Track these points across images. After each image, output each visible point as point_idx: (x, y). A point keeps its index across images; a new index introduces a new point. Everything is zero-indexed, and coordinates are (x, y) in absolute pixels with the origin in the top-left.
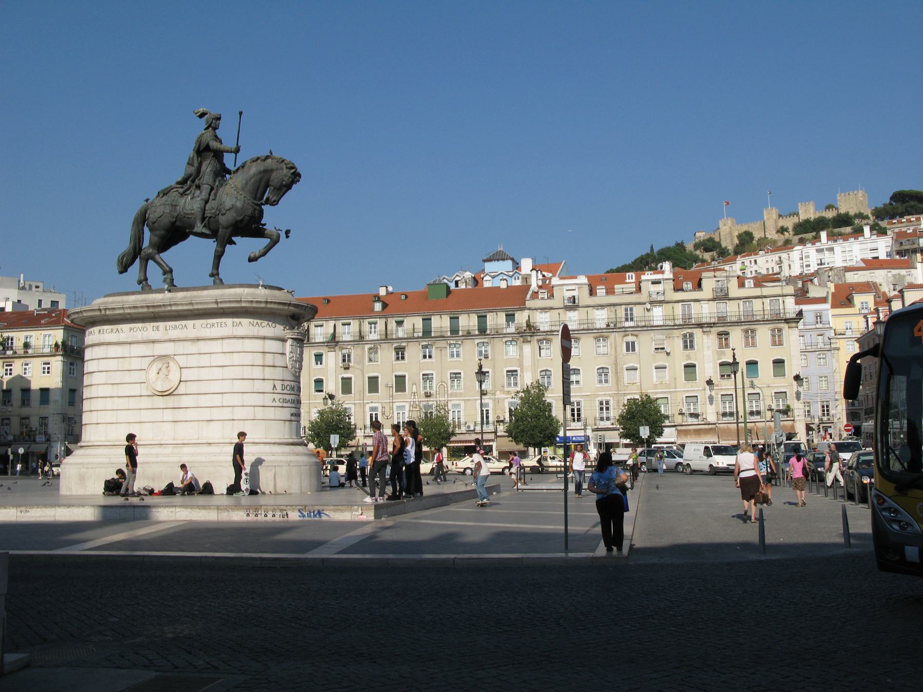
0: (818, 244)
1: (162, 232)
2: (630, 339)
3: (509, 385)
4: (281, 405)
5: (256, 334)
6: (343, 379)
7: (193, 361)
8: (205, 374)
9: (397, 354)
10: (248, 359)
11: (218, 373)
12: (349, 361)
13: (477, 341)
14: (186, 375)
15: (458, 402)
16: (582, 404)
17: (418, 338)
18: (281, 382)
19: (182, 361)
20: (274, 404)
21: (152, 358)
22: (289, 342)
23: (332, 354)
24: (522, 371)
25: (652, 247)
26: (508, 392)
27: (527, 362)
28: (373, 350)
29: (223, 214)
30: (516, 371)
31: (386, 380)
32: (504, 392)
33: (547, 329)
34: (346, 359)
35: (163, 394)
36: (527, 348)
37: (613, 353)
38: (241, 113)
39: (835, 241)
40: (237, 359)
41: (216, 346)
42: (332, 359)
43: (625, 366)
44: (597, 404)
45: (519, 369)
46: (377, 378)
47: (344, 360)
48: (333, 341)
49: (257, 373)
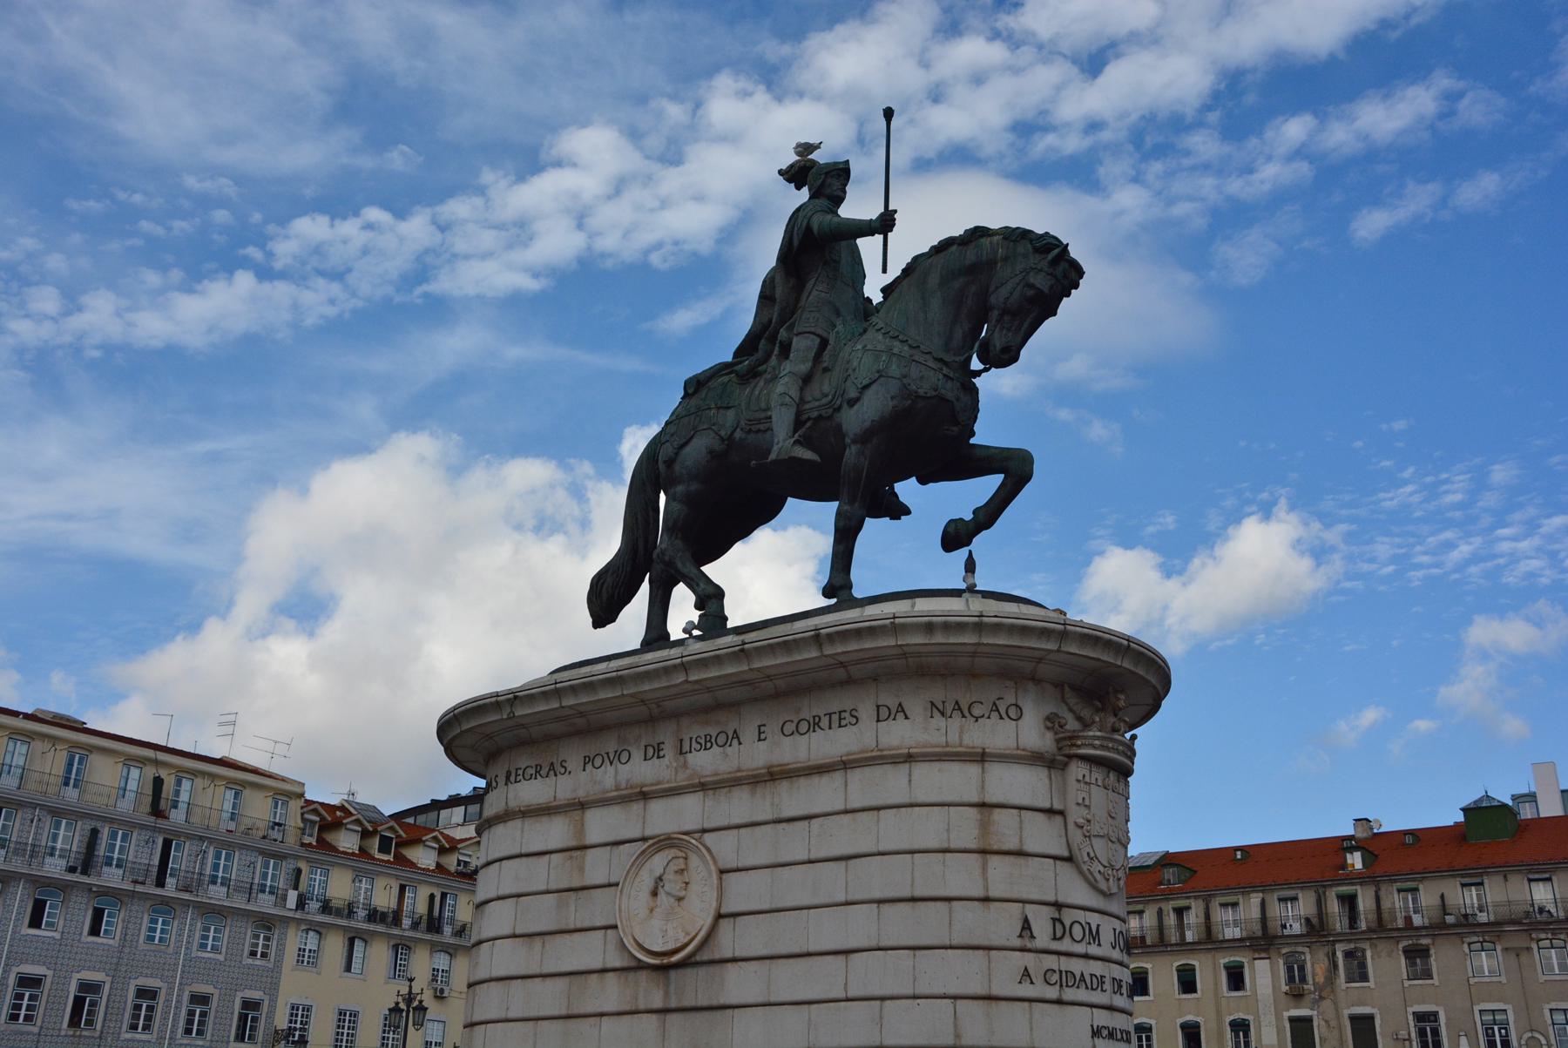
1: (694, 486)
4: (1052, 993)
5: (953, 737)
7: (757, 847)
8: (795, 887)
10: (927, 829)
11: (832, 882)
12: (1303, 979)
14: (745, 892)
18: (1048, 912)
19: (725, 847)
20: (1026, 990)
21: (640, 847)
22: (1078, 770)
23: (1262, 966)
29: (852, 403)
35: (665, 966)
38: (889, 114)
40: (893, 831)
41: (823, 794)
46: (1370, 1018)
47: (1291, 979)
48: (1264, 941)
49: (960, 876)
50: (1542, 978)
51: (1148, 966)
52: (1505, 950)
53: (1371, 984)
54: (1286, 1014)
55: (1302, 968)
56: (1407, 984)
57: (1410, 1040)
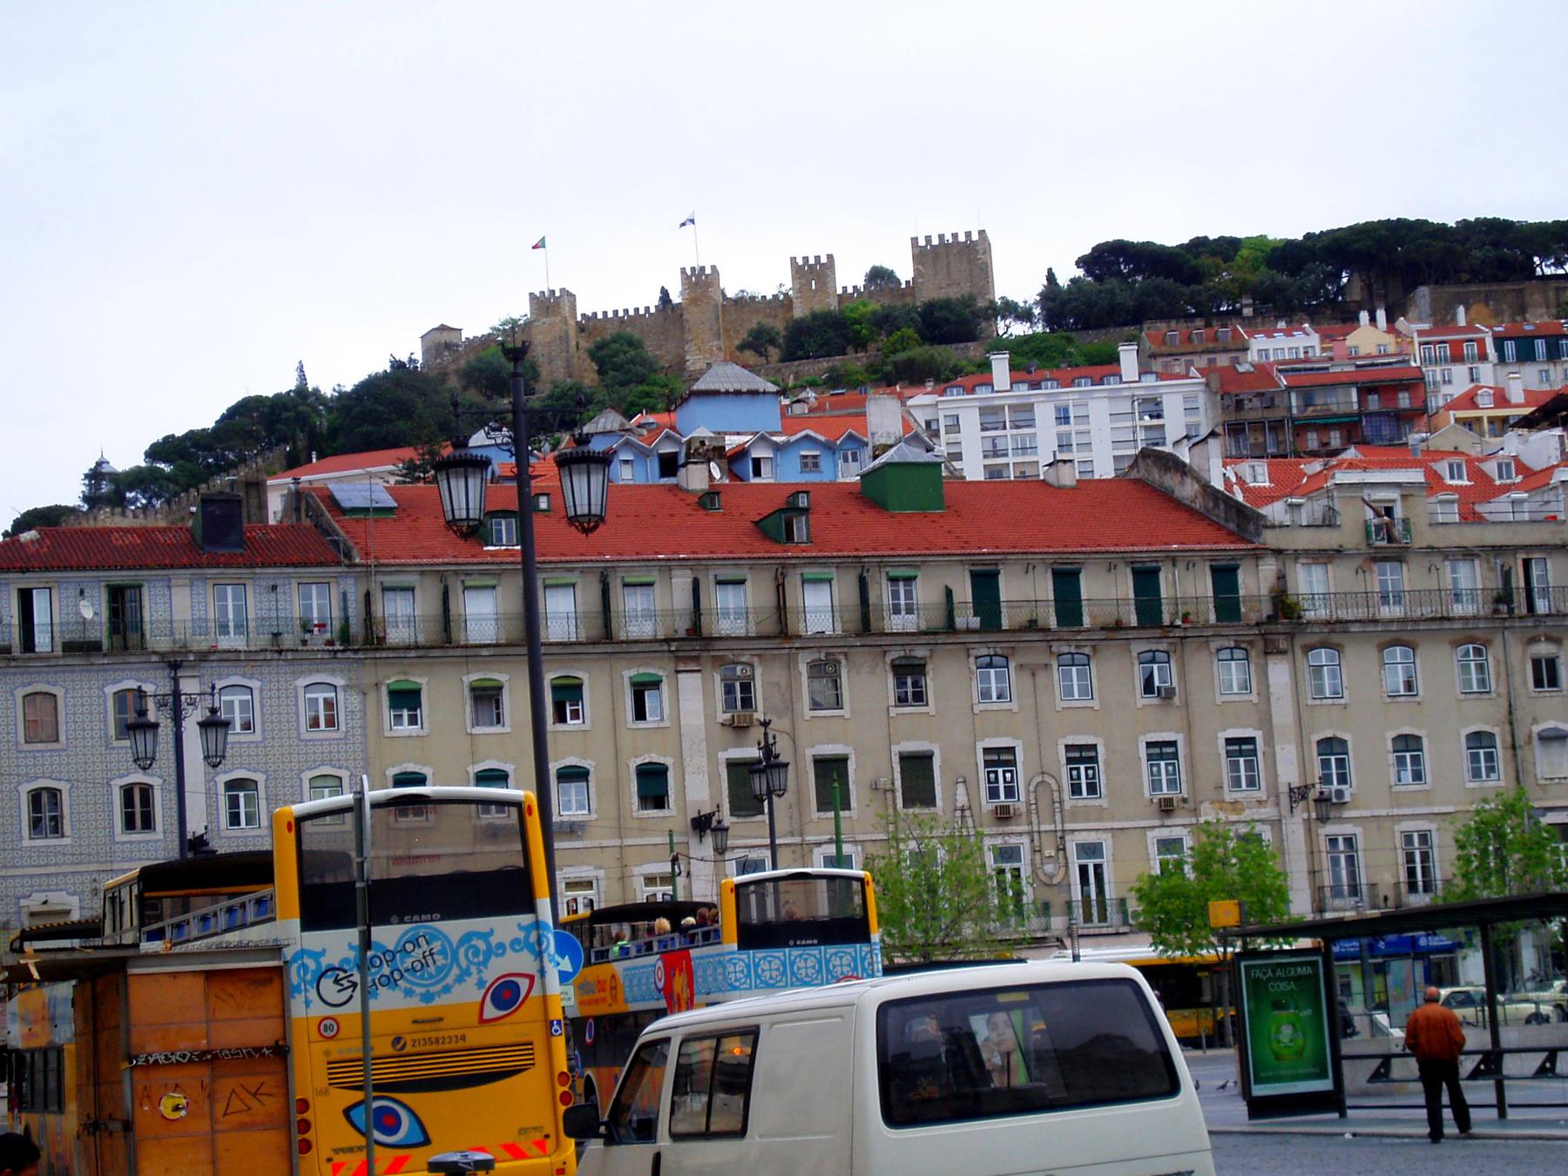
0: (982, 393)
2: (1544, 649)
3: (1236, 782)
6: (732, 765)
9: (901, 684)
13: (1137, 648)
15: (1091, 838)
16: (1360, 844)
17: (969, 631)
23: (690, 684)
24: (1270, 741)
25: (301, 369)
26: (1235, 806)
27: (1283, 713)
28: (826, 670)
30: (1251, 740)
31: (871, 768)
32: (1220, 803)
33: (1323, 614)
34: (741, 695)
36: (1279, 672)
37: (1503, 690)
39: (1035, 385)
42: (692, 700)
43: (1536, 729)
44: (1399, 841)
45: (1258, 735)
48: (693, 643)
50: (1060, 705)
51: (502, 678)
52: (1021, 667)
53: (845, 712)
54: (723, 756)
55: (746, 688)
56: (894, 712)
57: (893, 791)
